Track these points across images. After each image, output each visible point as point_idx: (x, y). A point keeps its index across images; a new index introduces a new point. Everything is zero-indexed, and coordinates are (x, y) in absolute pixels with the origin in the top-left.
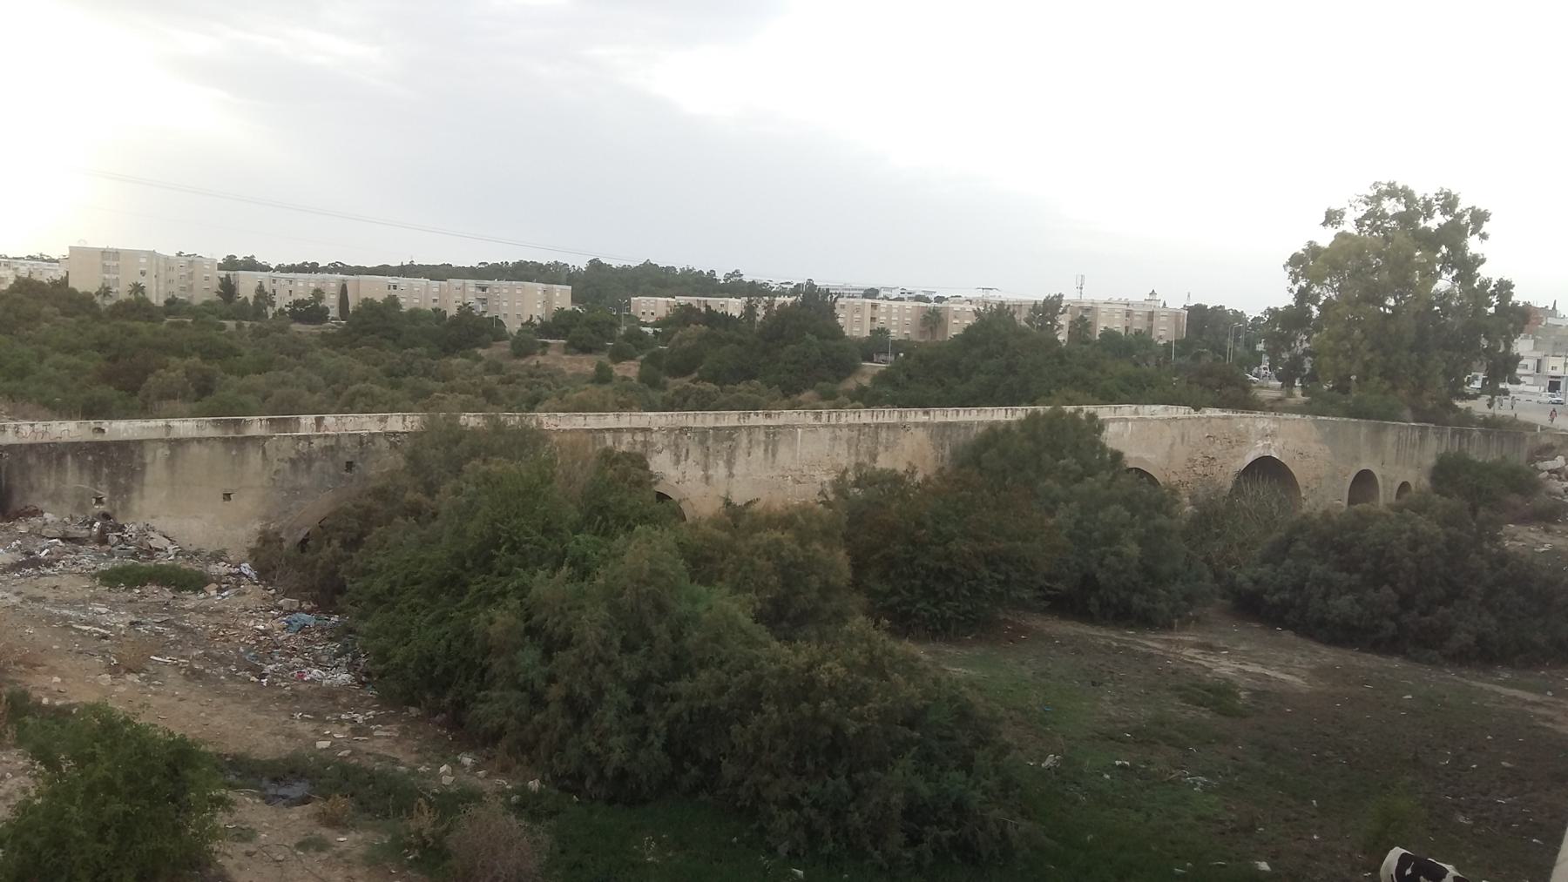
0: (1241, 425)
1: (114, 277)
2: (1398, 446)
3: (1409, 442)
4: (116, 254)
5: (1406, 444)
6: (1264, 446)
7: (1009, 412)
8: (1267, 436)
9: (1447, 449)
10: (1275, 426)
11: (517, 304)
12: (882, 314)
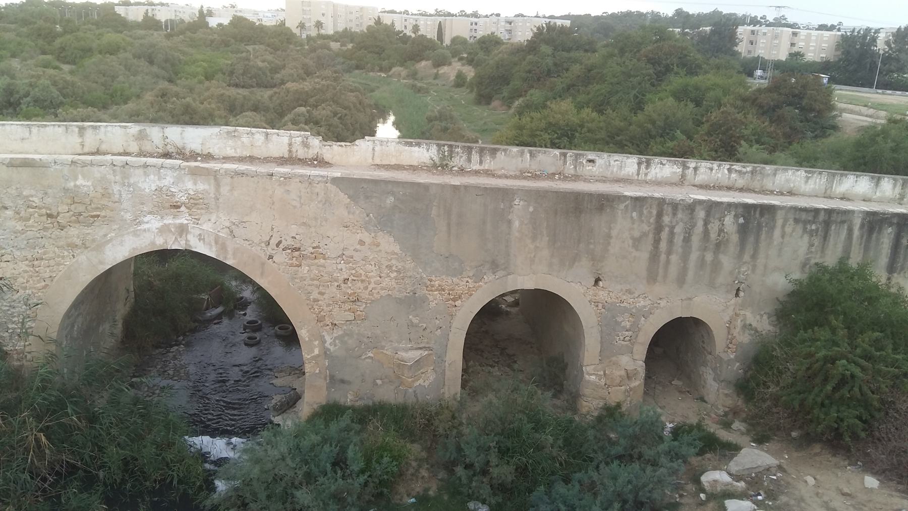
0: (80, 181)
1: (308, 17)
2: (657, 241)
3: (696, 240)
5: (687, 240)
6: (164, 230)
8: (179, 207)
9: (843, 261)
10: (201, 186)
11: (527, 33)
12: (803, 40)
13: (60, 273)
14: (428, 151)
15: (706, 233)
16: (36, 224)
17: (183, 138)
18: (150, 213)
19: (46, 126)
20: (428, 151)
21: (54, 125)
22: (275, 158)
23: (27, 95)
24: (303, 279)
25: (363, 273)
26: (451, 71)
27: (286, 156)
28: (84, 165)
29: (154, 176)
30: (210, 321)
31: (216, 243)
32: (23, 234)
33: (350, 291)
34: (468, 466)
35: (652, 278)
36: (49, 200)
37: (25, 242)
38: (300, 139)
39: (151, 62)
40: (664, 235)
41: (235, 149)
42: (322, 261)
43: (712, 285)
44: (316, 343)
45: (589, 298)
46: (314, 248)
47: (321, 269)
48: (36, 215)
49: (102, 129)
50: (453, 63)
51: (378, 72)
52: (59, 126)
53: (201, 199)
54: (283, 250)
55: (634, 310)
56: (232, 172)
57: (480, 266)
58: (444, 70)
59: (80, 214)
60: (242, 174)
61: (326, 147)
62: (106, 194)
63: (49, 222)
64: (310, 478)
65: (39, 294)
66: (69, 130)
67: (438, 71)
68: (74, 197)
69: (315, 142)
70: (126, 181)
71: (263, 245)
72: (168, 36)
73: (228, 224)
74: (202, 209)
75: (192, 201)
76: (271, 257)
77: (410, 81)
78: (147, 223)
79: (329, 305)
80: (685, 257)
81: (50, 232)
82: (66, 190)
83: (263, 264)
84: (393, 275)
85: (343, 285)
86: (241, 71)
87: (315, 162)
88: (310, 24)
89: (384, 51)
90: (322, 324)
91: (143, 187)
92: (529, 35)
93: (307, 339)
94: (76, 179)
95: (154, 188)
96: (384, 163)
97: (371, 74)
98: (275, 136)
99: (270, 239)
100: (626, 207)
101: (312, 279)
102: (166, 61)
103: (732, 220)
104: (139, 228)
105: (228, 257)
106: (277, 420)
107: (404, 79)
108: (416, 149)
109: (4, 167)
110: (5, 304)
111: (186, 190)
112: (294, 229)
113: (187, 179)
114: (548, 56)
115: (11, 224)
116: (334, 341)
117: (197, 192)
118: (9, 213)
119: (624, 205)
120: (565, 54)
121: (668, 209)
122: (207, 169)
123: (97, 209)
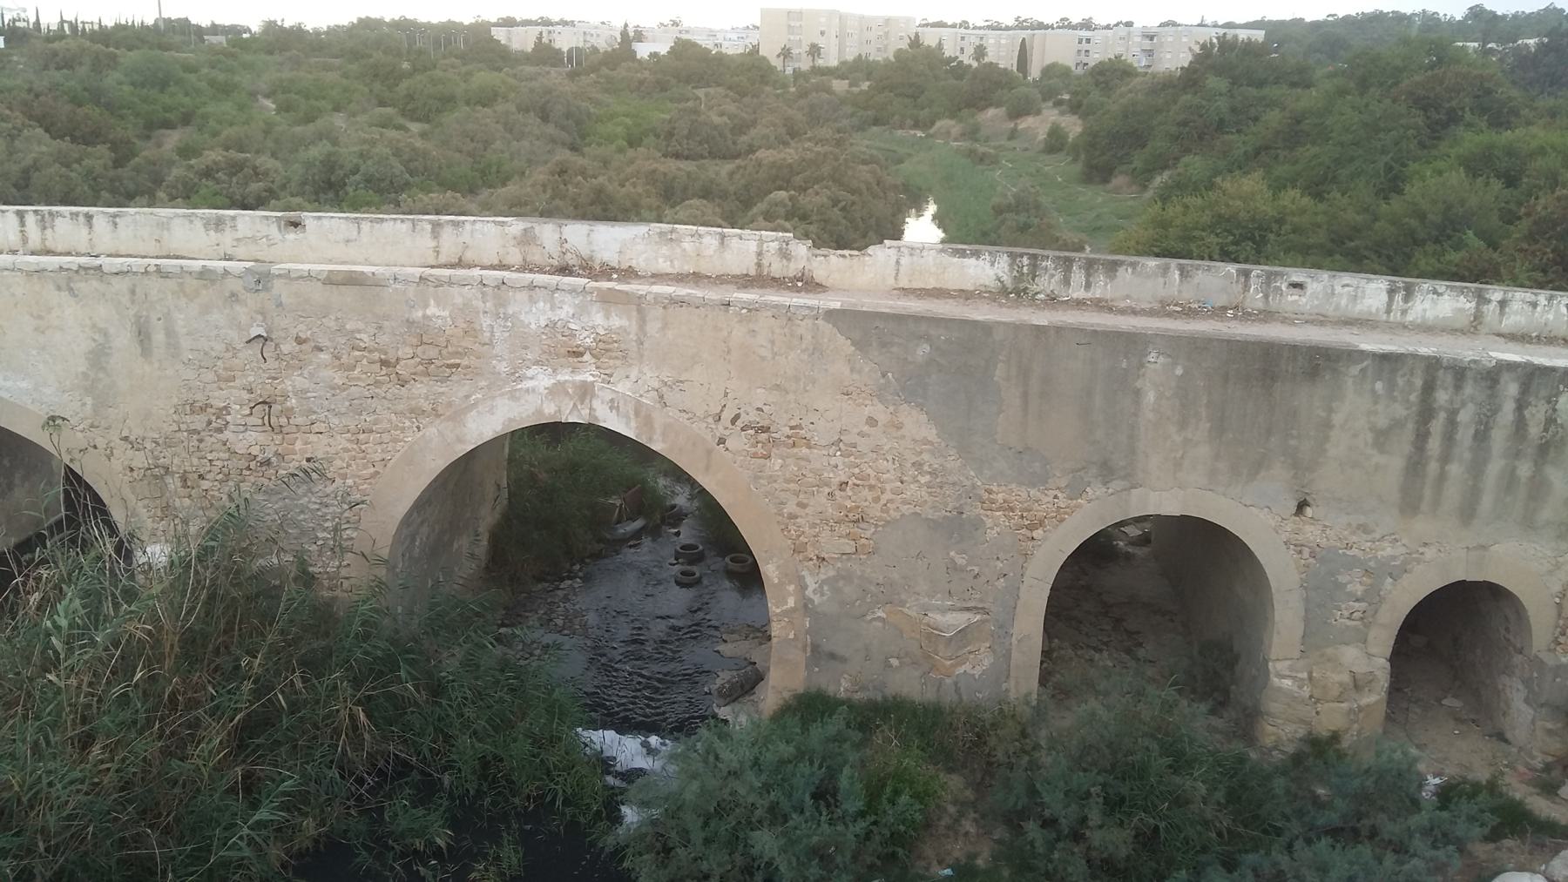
0: (432, 310)
2: (1422, 437)
3: (1499, 437)
4: (800, 14)
5: (1482, 435)
6: (556, 391)
7: (31, 220)
8: (581, 354)
10: (617, 322)
13: (398, 455)
14: (992, 264)
15: (1520, 424)
16: (364, 376)
17: (590, 243)
18: (537, 363)
19: (382, 220)
20: (992, 264)
21: (395, 219)
22: (733, 276)
23: (355, 171)
24: (772, 479)
25: (873, 474)
26: (1038, 125)
27: (753, 272)
28: (439, 283)
29: (544, 302)
30: (624, 541)
31: (637, 414)
32: (344, 390)
33: (849, 504)
34: (1049, 823)
35: (1410, 505)
36: (384, 339)
37: (347, 403)
38: (775, 245)
39: (545, 118)
40: (1437, 426)
41: (671, 261)
42: (805, 450)
43: (1528, 524)
44: (791, 588)
45: (1284, 537)
46: (792, 428)
47: (803, 463)
48: (365, 362)
49: (468, 227)
50: (1044, 111)
51: (911, 129)
52: (402, 221)
53: (616, 342)
54: (742, 430)
55: (1372, 564)
56: (666, 298)
57: (1079, 470)
58: (1027, 123)
59: (430, 362)
60: (681, 302)
61: (819, 258)
62: (471, 331)
63: (383, 372)
64: (776, 816)
65: (365, 486)
66: (418, 227)
67: (1016, 124)
68: (421, 334)
69: (801, 249)
70: (501, 310)
71: (710, 420)
72: (573, 75)
73: (656, 384)
74: (617, 358)
75: (601, 345)
76: (722, 441)
77: (964, 144)
78: (532, 378)
79: (814, 525)
80: (1477, 469)
81: (384, 389)
82: (410, 323)
83: (709, 452)
84: (924, 479)
85: (837, 493)
86: (685, 132)
87: (800, 284)
88: (800, 50)
89: (923, 92)
90: (801, 557)
91: (526, 322)
92: (1185, 59)
93: (776, 581)
94: (426, 306)
95: (543, 324)
96: (915, 285)
97: (900, 132)
98: (735, 240)
99: (722, 411)
101: (788, 481)
102: (568, 116)
104: (519, 386)
105: (655, 438)
106: (724, 712)
107: (956, 140)
108: (973, 261)
109: (319, 283)
110: (313, 499)
111: (593, 327)
112: (760, 396)
113: (595, 308)
114: (1221, 95)
115: (327, 373)
116: (821, 587)
117: (609, 330)
118: (324, 356)
119: (1359, 367)
120: (1253, 91)
121: (1445, 378)
122: (627, 293)
123: (456, 354)
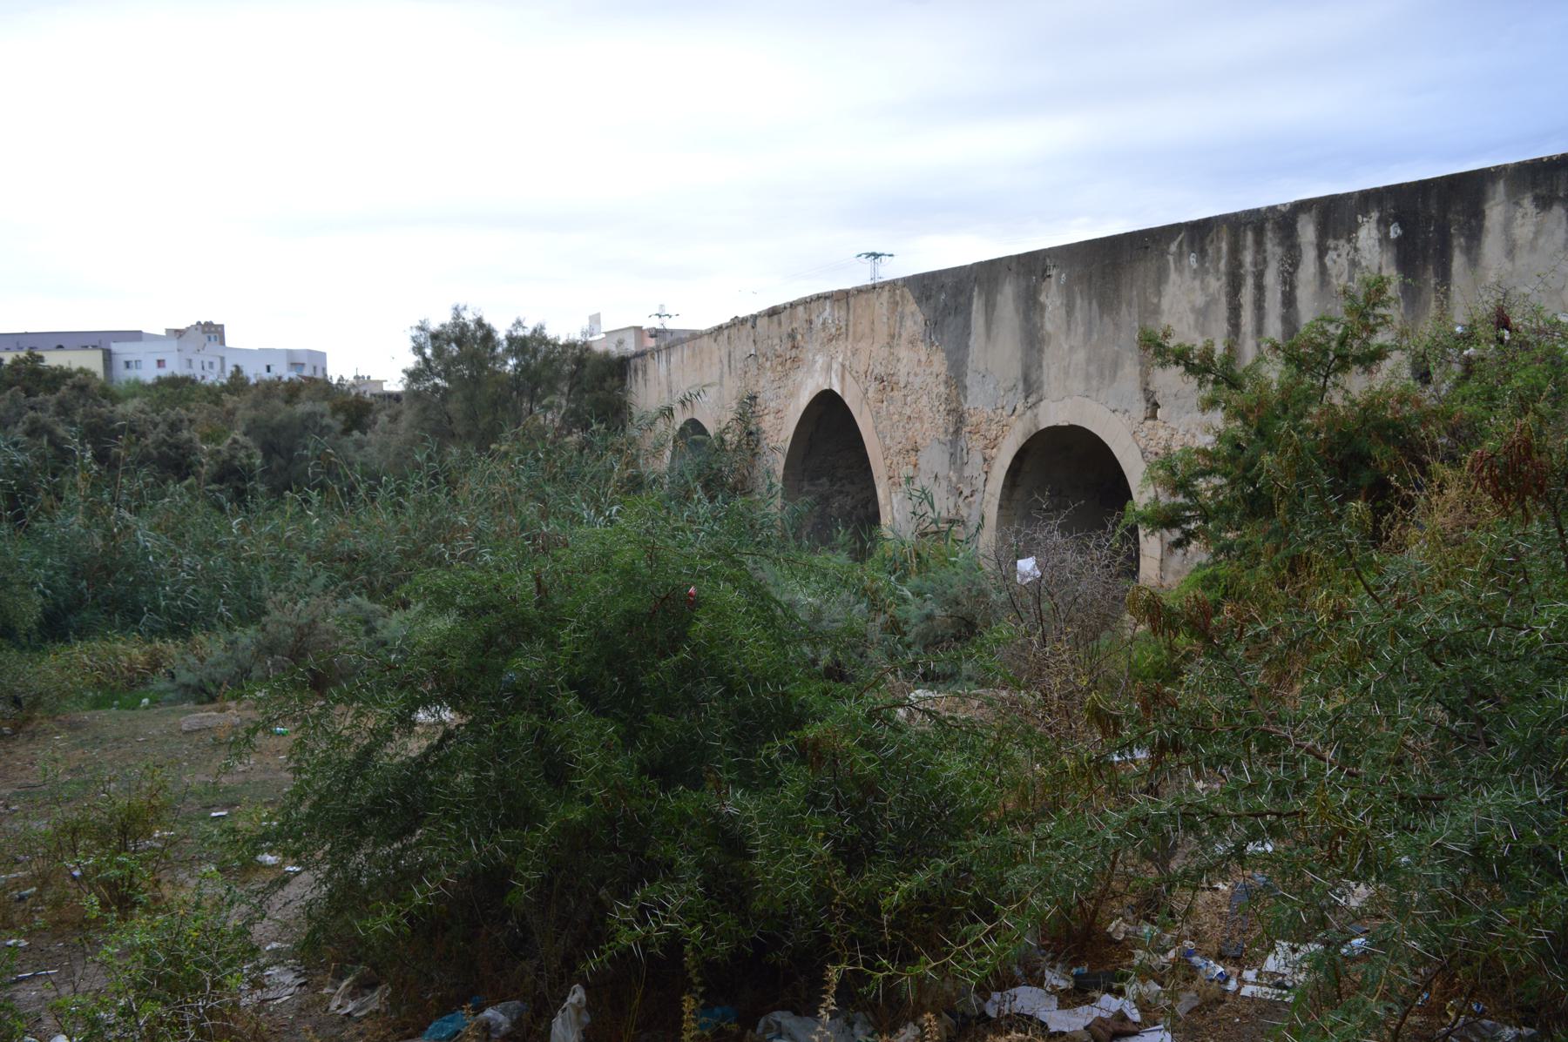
40: (1247, 295)
100: (1180, 245)
103: (1374, 233)
119: (1176, 243)
